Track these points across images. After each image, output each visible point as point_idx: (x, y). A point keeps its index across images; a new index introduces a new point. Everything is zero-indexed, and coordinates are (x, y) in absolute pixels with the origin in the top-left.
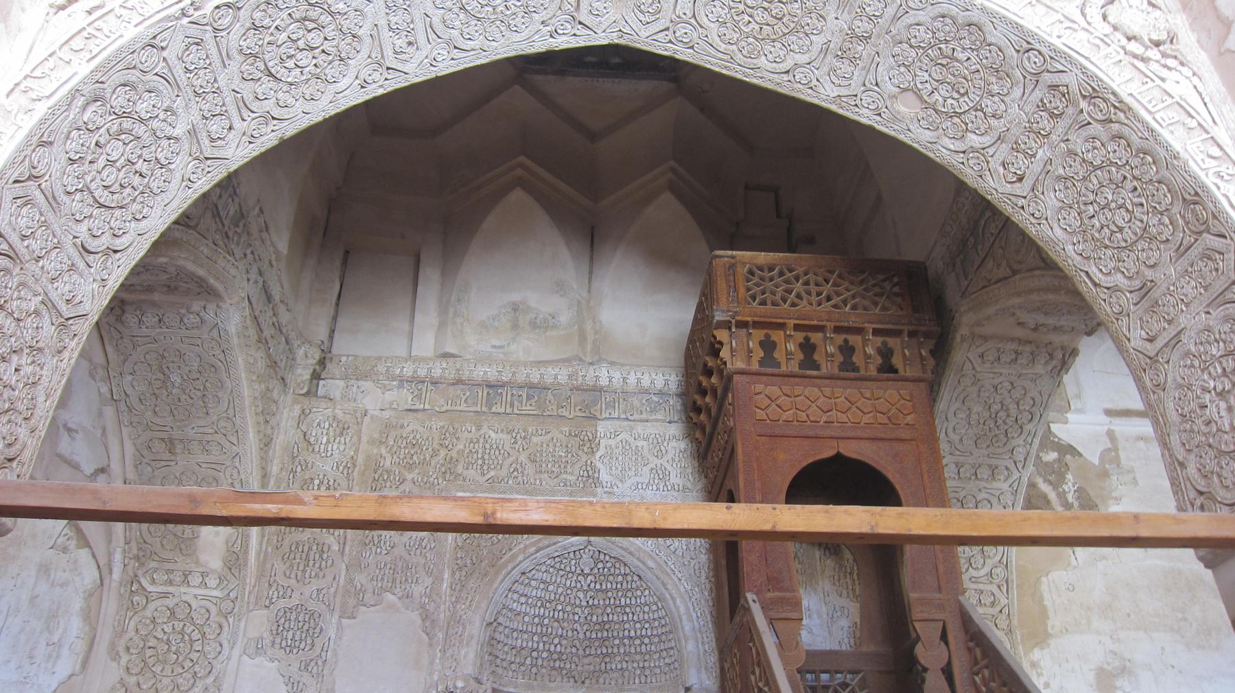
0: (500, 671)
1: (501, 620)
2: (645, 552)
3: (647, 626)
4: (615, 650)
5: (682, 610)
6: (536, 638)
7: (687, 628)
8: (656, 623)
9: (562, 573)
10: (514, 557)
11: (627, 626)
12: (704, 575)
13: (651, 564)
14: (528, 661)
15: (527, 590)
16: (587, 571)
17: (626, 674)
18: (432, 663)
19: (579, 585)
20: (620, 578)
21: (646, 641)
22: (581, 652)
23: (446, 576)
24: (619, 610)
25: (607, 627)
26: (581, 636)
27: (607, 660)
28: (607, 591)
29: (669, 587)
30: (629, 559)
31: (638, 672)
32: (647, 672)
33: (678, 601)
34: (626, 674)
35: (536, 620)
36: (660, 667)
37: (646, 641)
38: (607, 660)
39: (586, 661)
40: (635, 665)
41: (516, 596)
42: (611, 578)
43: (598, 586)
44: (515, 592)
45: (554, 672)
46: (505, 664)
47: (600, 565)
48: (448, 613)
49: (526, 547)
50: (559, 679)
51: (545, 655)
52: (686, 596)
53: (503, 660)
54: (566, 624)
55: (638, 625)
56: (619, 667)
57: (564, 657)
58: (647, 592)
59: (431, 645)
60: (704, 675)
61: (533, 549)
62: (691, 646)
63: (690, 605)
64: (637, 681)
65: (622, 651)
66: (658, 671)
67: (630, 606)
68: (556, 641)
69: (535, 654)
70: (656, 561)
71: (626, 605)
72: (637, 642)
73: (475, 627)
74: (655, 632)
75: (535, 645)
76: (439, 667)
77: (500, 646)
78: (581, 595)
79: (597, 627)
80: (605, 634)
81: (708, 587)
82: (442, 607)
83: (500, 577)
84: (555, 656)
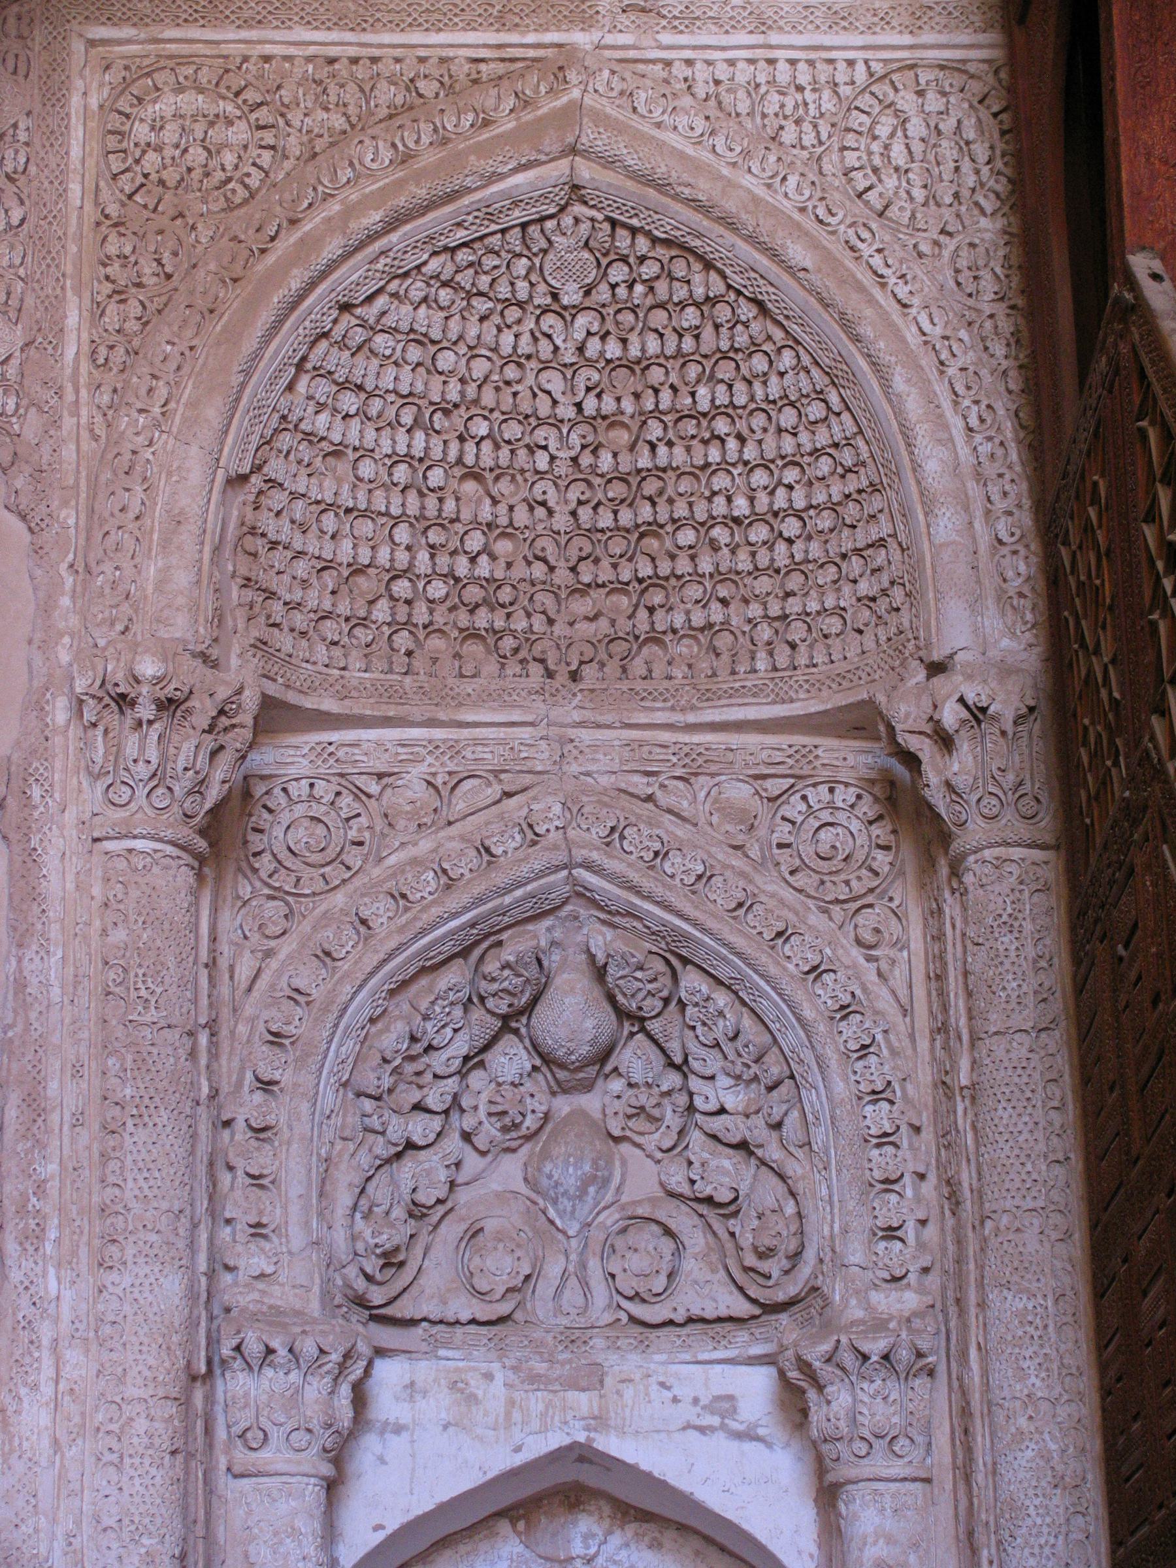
0: (284, 641)
1: (276, 468)
2: (774, 212)
3: (791, 475)
4: (683, 565)
5: (913, 406)
6: (402, 534)
7: (931, 467)
8: (824, 466)
9: (482, 305)
10: (310, 244)
11: (720, 481)
12: (989, 286)
13: (798, 253)
14: (381, 611)
15: (364, 369)
16: (571, 295)
17: (724, 641)
18: (46, 608)
19: (545, 348)
20: (691, 316)
21: (791, 527)
22: (562, 576)
23: (72, 320)
24: (690, 427)
25: (651, 487)
26: (561, 521)
27: (657, 598)
28: (641, 365)
29: (867, 331)
30: (720, 242)
31: (765, 632)
32: (797, 632)
33: (899, 383)
34: (724, 641)
35: (401, 473)
36: (840, 611)
37: (791, 527)
38: (657, 598)
39: (581, 606)
40: (755, 610)
41: (323, 389)
42: (658, 318)
43: (613, 349)
44: (320, 373)
45: (473, 648)
46: (299, 620)
47: (618, 273)
48: (87, 445)
49: (349, 212)
50: (491, 667)
51: (438, 589)
52: (927, 362)
53: (293, 606)
54: (504, 486)
55: (760, 478)
56: (698, 619)
57: (505, 595)
58: (787, 359)
59: (37, 550)
60: (992, 621)
61: (374, 217)
62: (946, 525)
63: (941, 391)
64: (761, 665)
65: (706, 566)
66: (833, 624)
67: (729, 411)
68: (475, 542)
69: (402, 588)
70: (815, 245)
71: (717, 411)
72: (759, 533)
73: (186, 478)
74: (820, 498)
75: (402, 557)
76: (74, 621)
77: (279, 558)
78: (554, 382)
79: (617, 490)
80: (646, 512)
81: (1006, 327)
82: (68, 422)
83: (265, 317)
84: (473, 593)
